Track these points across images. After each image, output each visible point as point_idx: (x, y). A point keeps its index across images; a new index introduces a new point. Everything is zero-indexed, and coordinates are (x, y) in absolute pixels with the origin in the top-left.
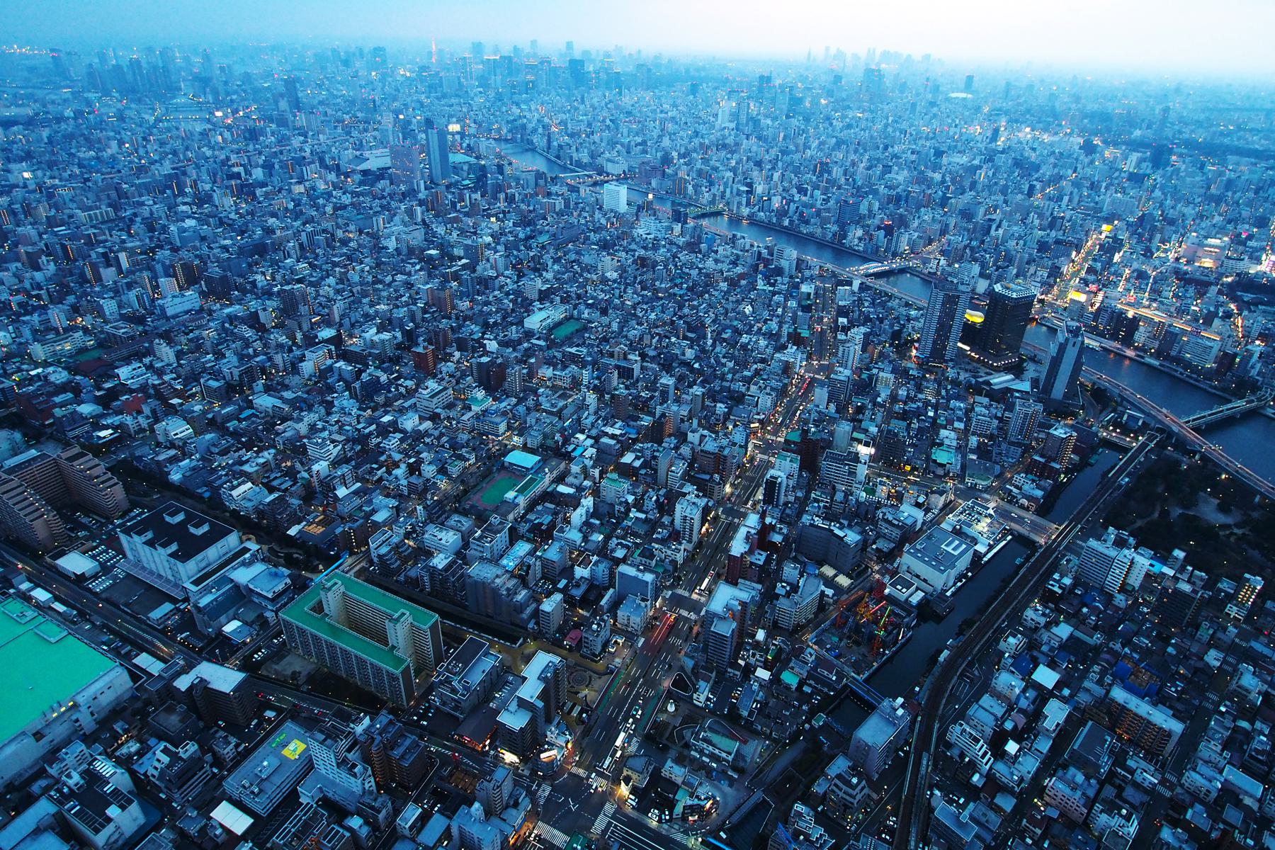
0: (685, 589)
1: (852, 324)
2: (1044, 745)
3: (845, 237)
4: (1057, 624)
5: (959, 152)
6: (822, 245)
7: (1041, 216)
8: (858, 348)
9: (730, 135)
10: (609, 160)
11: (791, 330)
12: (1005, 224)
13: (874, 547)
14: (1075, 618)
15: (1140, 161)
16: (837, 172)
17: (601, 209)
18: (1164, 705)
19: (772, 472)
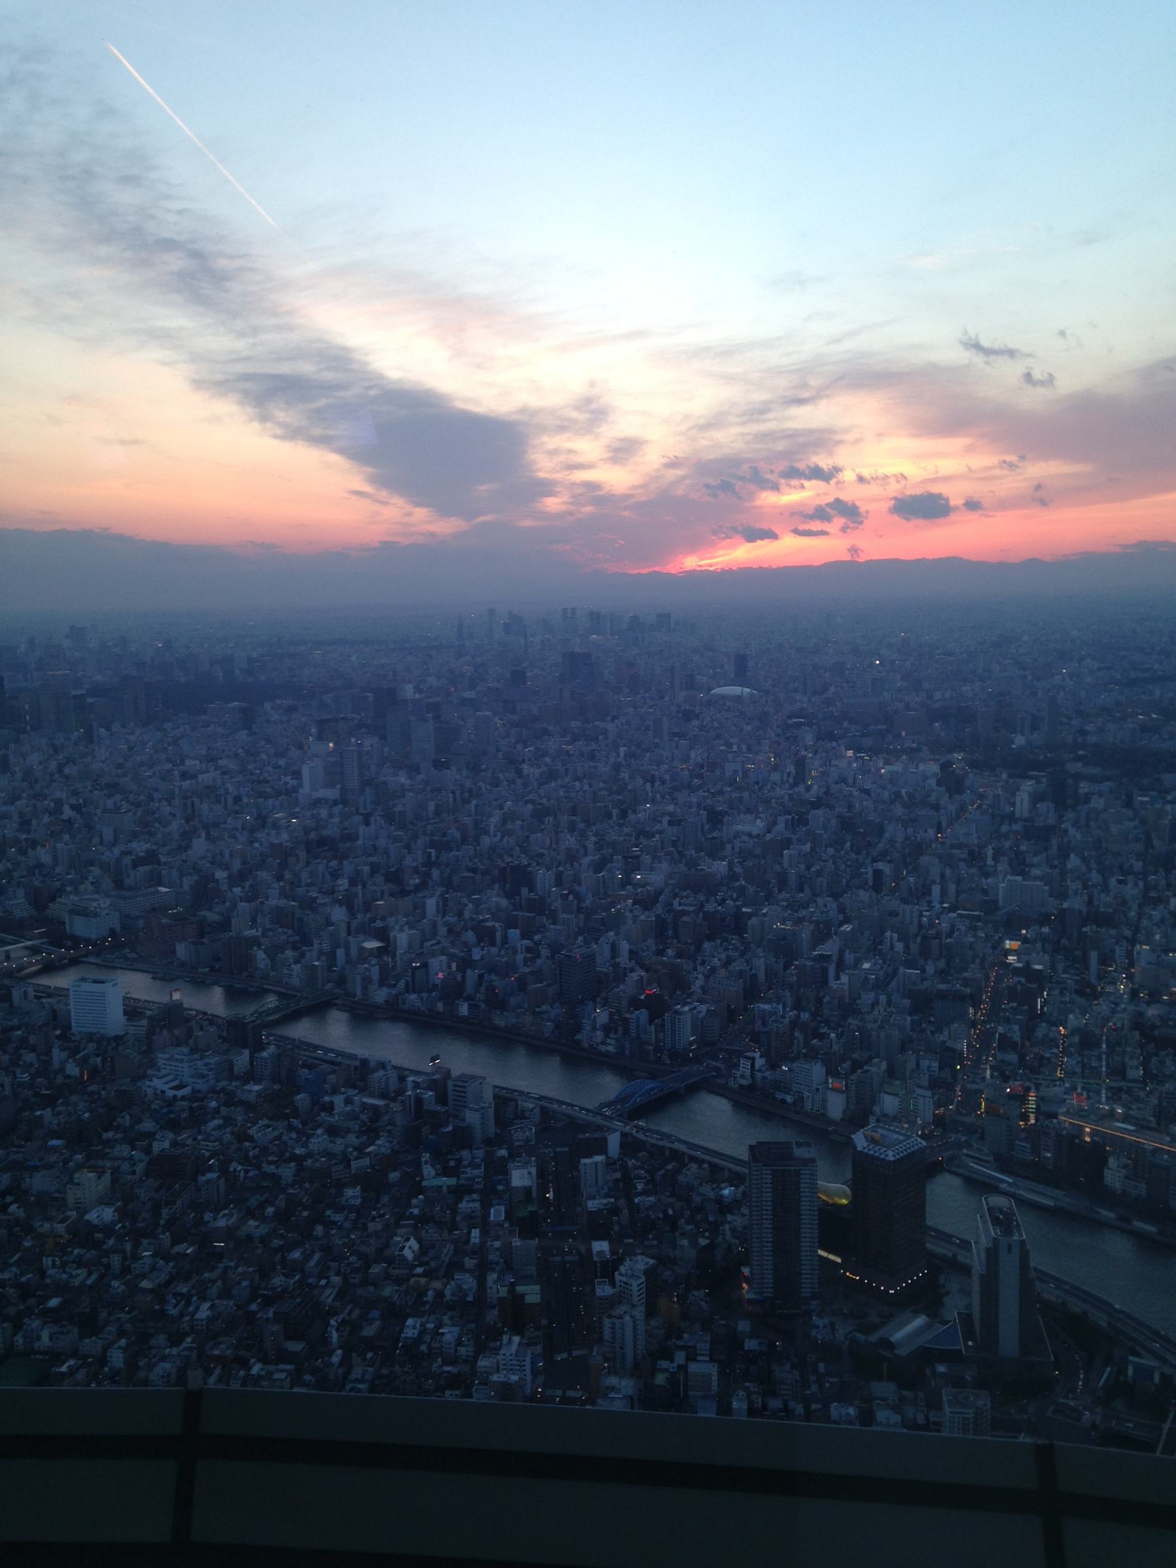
5: (749, 811)
6: (538, 1048)
7: (904, 938)
8: (639, 1312)
9: (331, 816)
10: (74, 912)
15: (1037, 798)
17: (64, 1037)
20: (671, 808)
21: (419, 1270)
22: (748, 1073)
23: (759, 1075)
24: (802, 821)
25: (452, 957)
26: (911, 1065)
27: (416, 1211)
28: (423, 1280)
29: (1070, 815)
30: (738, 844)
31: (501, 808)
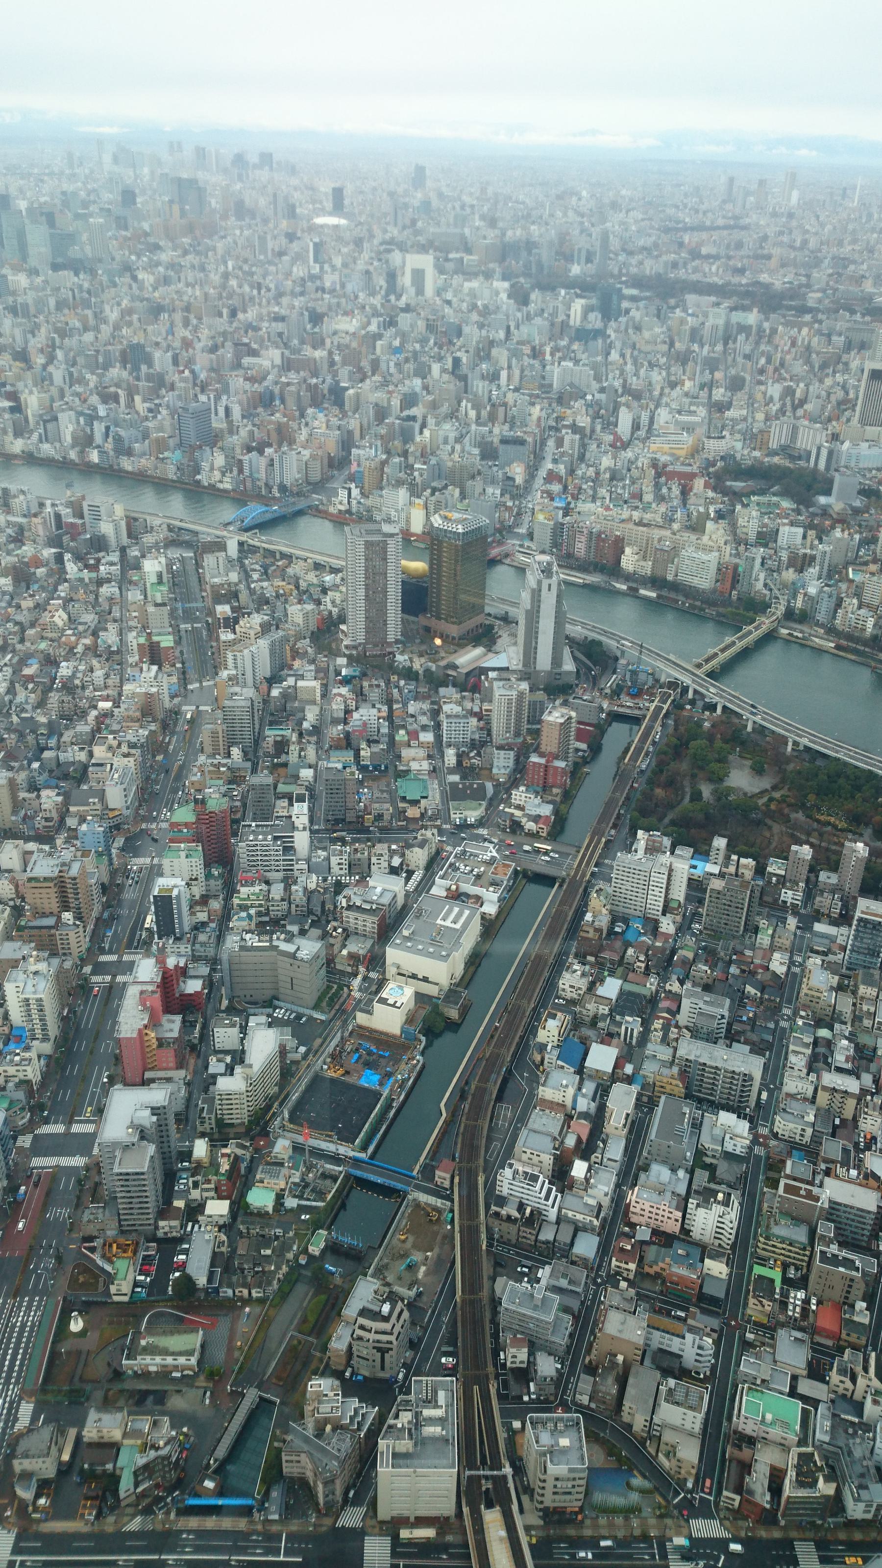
0: (56, 1122)
1: (239, 612)
2: (615, 1150)
3: (197, 470)
4: (602, 981)
5: (346, 313)
6: (162, 486)
7: (477, 407)
11: (142, 640)
12: (431, 421)
13: (345, 952)
14: (620, 967)
15: (587, 310)
16: (161, 360)
18: (739, 1041)
19: (161, 883)
20: (276, 309)
21: (69, 632)
22: (345, 501)
23: (354, 502)
24: (391, 323)
25: (80, 414)
26: (478, 490)
27: (63, 594)
28: (73, 638)
29: (612, 324)
30: (336, 340)
31: (119, 304)
